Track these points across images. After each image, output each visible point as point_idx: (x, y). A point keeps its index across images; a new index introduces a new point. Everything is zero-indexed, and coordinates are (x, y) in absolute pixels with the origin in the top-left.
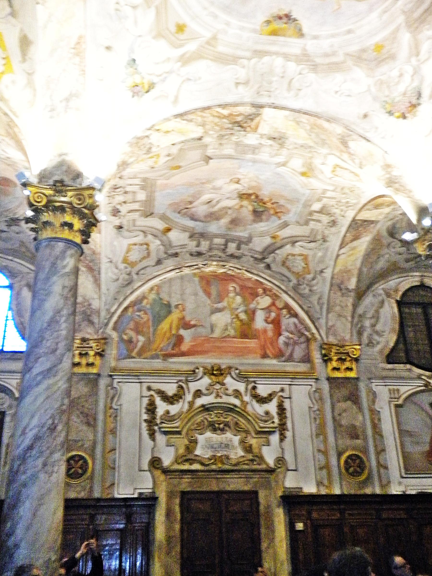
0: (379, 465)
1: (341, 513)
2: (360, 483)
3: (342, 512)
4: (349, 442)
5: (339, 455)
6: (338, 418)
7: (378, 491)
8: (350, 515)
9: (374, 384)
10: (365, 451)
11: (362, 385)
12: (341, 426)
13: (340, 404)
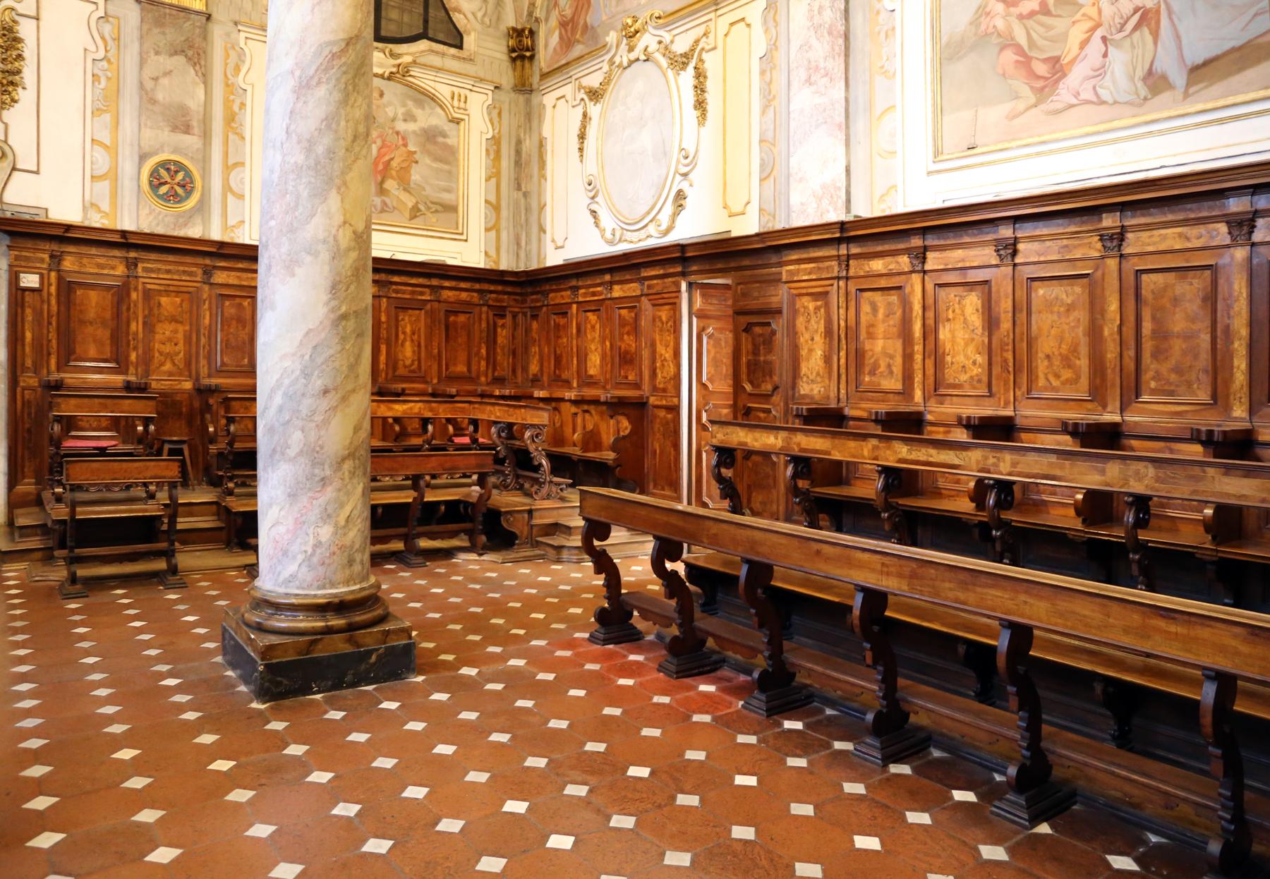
0: (227, 188)
1: (128, 267)
2: (179, 216)
3: (132, 264)
4: (166, 136)
5: (143, 158)
6: (149, 85)
7: (216, 235)
8: (145, 269)
9: (243, 35)
10: (205, 161)
11: (218, 32)
12: (153, 101)
13: (161, 58)
